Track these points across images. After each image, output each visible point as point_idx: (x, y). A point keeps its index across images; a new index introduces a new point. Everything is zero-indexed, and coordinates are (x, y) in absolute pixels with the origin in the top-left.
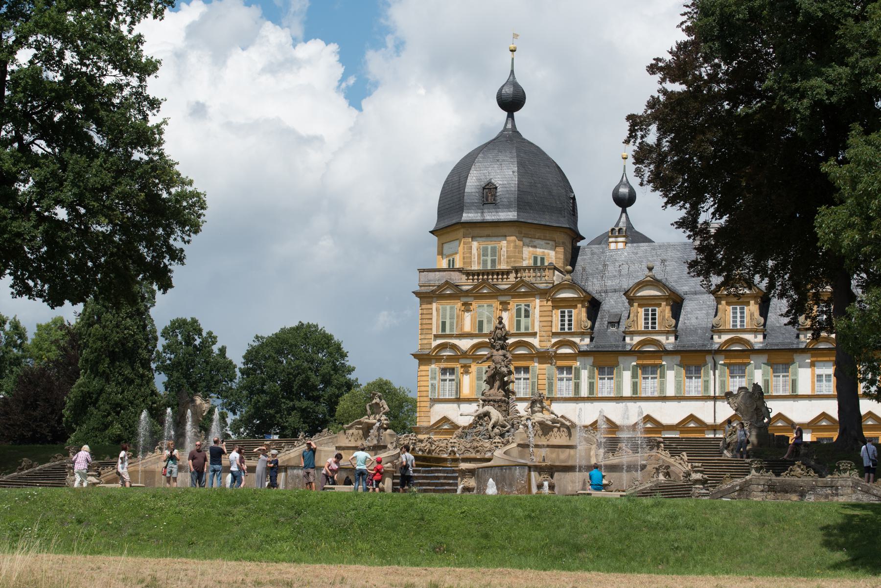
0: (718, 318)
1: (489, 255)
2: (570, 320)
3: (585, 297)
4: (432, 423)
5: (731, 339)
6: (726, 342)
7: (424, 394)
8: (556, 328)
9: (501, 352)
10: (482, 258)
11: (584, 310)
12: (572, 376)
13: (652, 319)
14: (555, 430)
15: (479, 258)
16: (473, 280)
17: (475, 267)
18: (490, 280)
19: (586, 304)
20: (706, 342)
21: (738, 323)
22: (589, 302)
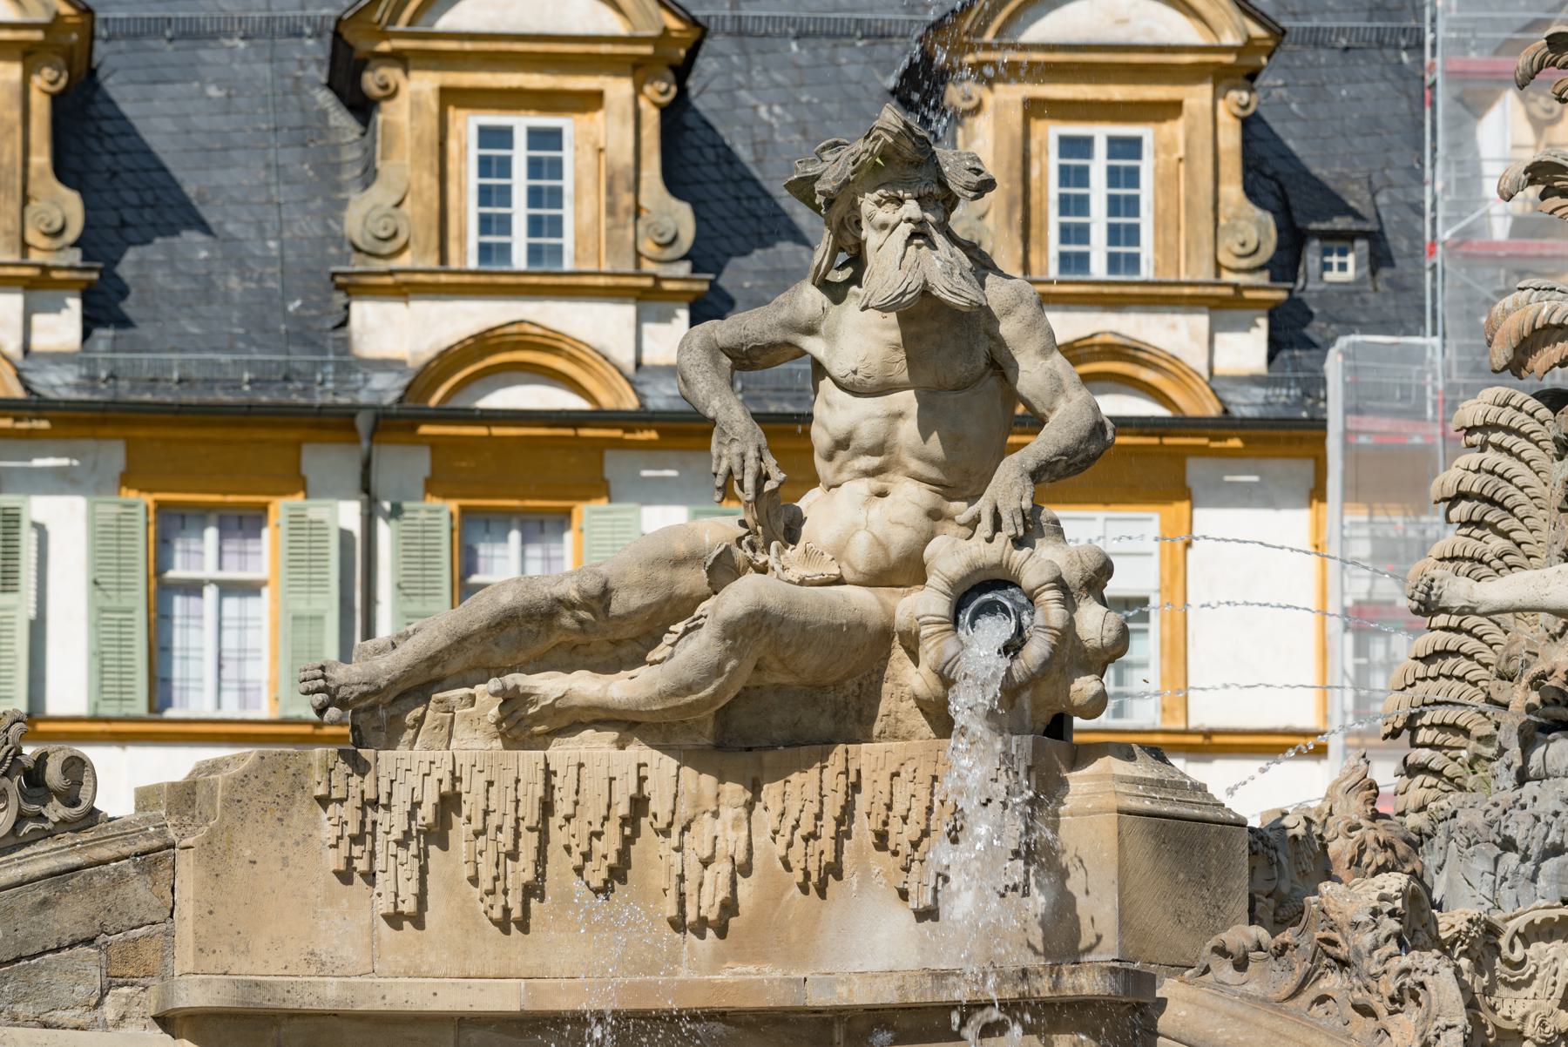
0: (380, 195)
5: (484, 342)
21: (519, 240)
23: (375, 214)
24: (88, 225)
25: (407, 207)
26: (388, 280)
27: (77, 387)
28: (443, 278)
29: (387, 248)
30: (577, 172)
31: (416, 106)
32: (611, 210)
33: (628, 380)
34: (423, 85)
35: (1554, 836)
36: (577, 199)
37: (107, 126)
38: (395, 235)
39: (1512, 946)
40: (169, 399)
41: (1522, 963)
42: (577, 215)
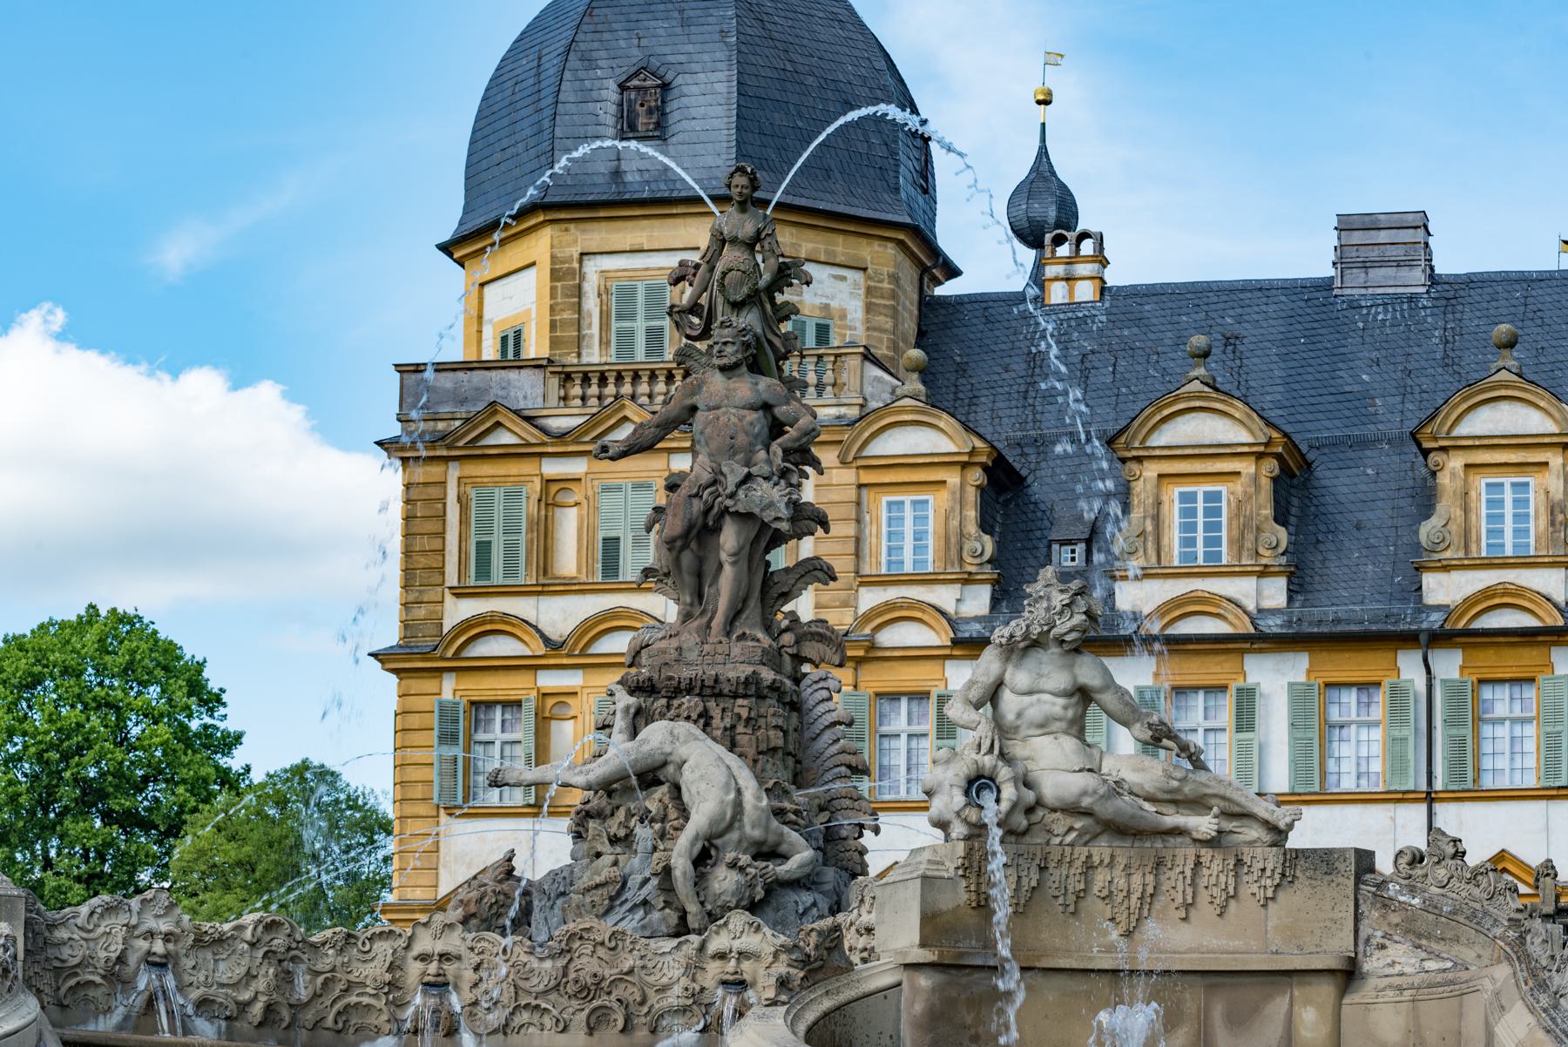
1: (639, 317)
2: (919, 536)
3: (973, 452)
4: (443, 890)
5: (1488, 593)
6: (1470, 602)
7: (418, 792)
8: (877, 563)
9: (745, 388)
10: (614, 325)
11: (972, 495)
12: (929, 725)
13: (1208, 527)
14: (1185, 854)
15: (605, 325)
16: (583, 398)
17: (593, 356)
18: (645, 400)
19: (976, 476)
20: (1396, 607)
21: (1508, 538)
22: (985, 468)
23: (1433, 531)
24: (1289, 543)
25: (1448, 527)
26: (1439, 565)
27: (1281, 626)
28: (1466, 562)
29: (1443, 546)
30: (1536, 504)
31: (1453, 475)
32: (1553, 523)
33: (1559, 609)
34: (1456, 462)
35: (562, 889)
36: (1537, 518)
37: (1315, 492)
38: (1443, 540)
39: (364, 943)
40: (1326, 630)
41: (370, 951)
42: (1536, 526)
